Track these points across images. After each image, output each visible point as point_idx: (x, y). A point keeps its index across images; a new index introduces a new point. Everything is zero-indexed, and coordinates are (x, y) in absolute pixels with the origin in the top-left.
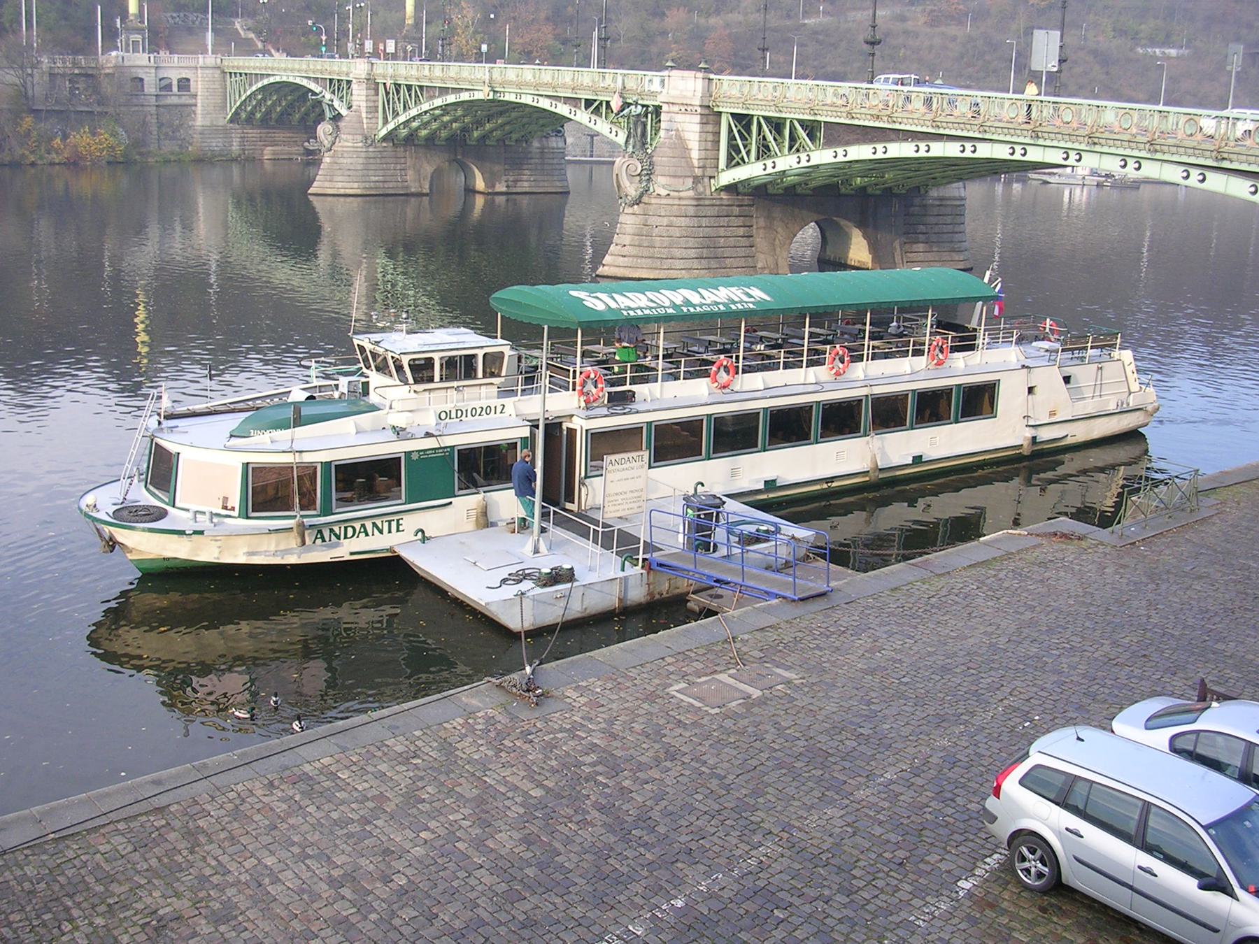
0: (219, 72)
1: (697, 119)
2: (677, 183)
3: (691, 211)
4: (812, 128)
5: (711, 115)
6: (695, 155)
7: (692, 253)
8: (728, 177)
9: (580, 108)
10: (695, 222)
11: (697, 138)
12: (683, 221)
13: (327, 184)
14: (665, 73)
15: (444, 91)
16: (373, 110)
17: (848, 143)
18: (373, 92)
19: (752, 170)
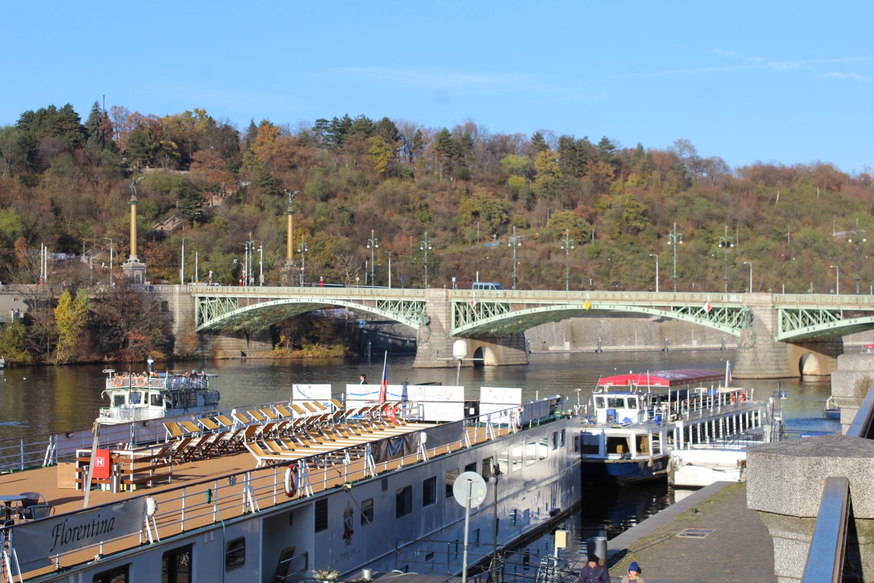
0: (189, 297)
1: (771, 312)
2: (765, 338)
3: (772, 350)
4: (834, 313)
5: (775, 311)
6: (769, 327)
7: (774, 367)
8: (783, 336)
9: (670, 310)
10: (772, 354)
11: (770, 320)
12: (769, 354)
13: (427, 362)
14: (745, 294)
15: (529, 306)
16: (449, 318)
17: (856, 317)
18: (448, 307)
19: (790, 334)
